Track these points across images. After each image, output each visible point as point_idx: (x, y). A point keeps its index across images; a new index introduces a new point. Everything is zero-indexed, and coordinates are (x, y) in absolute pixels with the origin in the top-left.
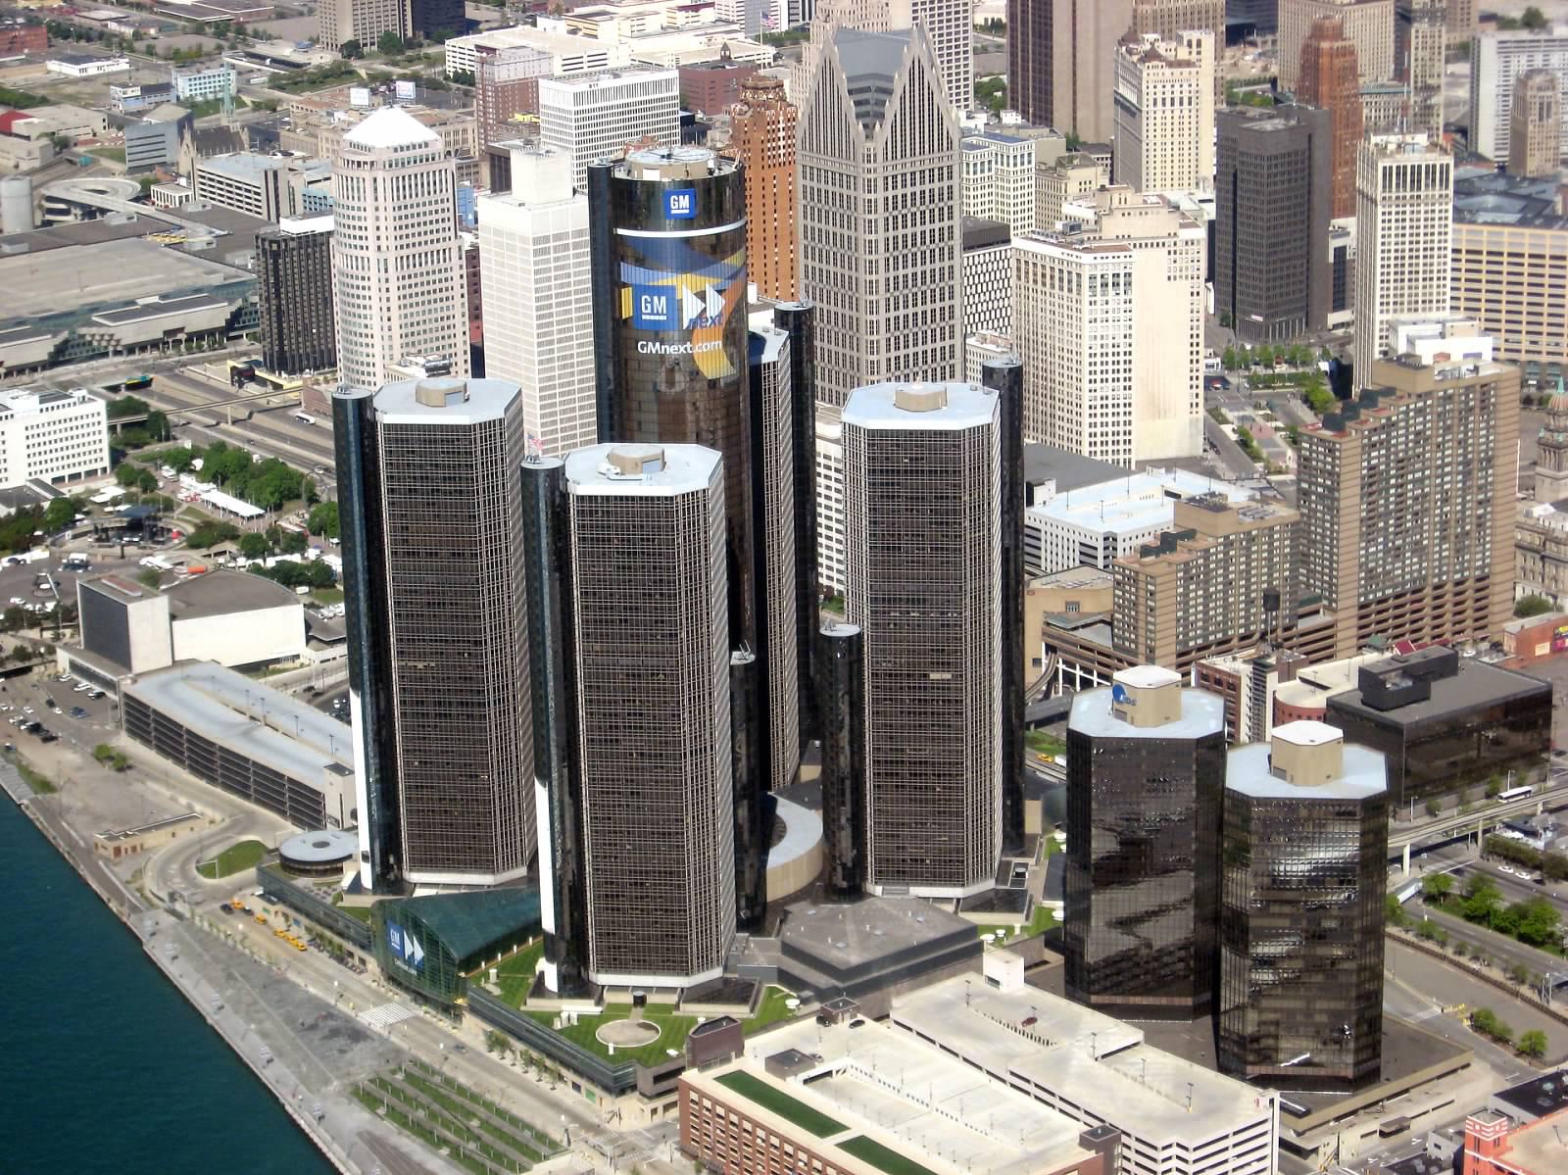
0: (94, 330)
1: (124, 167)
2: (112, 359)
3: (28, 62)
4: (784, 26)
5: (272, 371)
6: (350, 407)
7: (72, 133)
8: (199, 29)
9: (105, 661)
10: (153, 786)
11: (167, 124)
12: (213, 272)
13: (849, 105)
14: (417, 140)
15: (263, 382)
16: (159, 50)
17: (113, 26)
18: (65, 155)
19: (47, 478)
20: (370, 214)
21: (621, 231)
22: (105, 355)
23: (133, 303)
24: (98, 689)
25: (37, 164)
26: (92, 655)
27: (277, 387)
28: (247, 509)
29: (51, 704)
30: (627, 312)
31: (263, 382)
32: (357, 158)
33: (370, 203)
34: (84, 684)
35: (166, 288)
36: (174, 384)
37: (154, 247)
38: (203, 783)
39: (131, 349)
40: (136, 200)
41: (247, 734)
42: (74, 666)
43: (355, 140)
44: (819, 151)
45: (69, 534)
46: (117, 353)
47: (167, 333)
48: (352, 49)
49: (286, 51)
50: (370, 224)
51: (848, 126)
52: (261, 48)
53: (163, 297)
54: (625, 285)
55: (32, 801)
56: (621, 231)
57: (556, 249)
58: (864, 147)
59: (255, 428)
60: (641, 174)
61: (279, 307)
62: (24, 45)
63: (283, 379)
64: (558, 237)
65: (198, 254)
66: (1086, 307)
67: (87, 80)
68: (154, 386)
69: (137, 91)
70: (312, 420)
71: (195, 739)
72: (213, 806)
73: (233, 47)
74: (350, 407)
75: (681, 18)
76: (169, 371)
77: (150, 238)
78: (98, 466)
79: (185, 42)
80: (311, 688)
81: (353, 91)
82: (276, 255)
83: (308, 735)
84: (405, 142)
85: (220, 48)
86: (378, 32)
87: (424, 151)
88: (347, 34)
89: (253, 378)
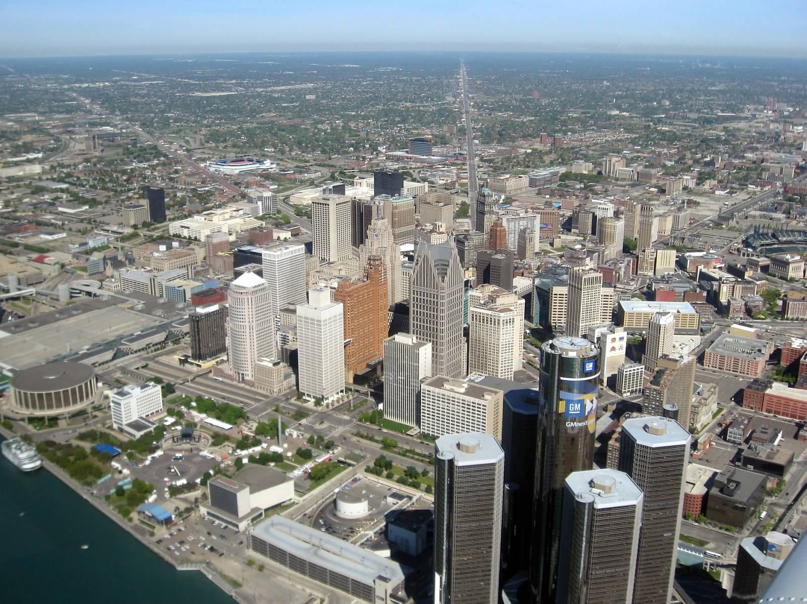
0: (124, 347)
1: (88, 274)
2: (130, 356)
3: (33, 235)
4: (261, 214)
5: (195, 359)
6: (446, 463)
7: (64, 262)
8: (82, 221)
9: (223, 512)
10: (279, 578)
11: (99, 260)
12: (155, 321)
13: (435, 271)
14: (260, 283)
15: (192, 364)
16: (74, 229)
17: (53, 221)
18: (64, 269)
19: (144, 416)
20: (246, 310)
21: (562, 378)
22: (128, 354)
23: (132, 335)
24: (224, 525)
25: (56, 274)
26: (213, 508)
27: (199, 366)
28: (227, 426)
29: (209, 534)
30: (562, 409)
31: (192, 364)
32: (240, 291)
33: (246, 306)
34: (217, 522)
35: (142, 329)
36: (156, 365)
37: (123, 309)
38: (298, 574)
39: (136, 352)
40: (100, 288)
41: (316, 554)
42: (209, 513)
43: (238, 284)
44: (434, 288)
45: (163, 440)
46: (132, 353)
47: (147, 345)
48: (135, 227)
49: (115, 228)
50: (246, 314)
51: (434, 278)
52: (106, 228)
53: (142, 331)
54: (561, 400)
55: (236, 593)
56: (562, 378)
57: (329, 323)
58: (441, 284)
59: (197, 383)
60: (567, 354)
61: (199, 339)
62: (28, 229)
63: (201, 363)
64: (330, 319)
65: (140, 311)
66: (501, 330)
67: (55, 240)
68: (149, 366)
69: (77, 246)
70: (221, 379)
71: (292, 557)
72: (319, 591)
73: (96, 228)
74: (446, 463)
75: (234, 214)
76: (153, 359)
77: (120, 305)
78: (159, 409)
79: (82, 226)
80: (305, 515)
81: (160, 246)
82: (198, 321)
83: (344, 553)
84: (257, 284)
85: (92, 228)
86: (142, 221)
87: (262, 287)
88: (132, 222)
89: (187, 362)
